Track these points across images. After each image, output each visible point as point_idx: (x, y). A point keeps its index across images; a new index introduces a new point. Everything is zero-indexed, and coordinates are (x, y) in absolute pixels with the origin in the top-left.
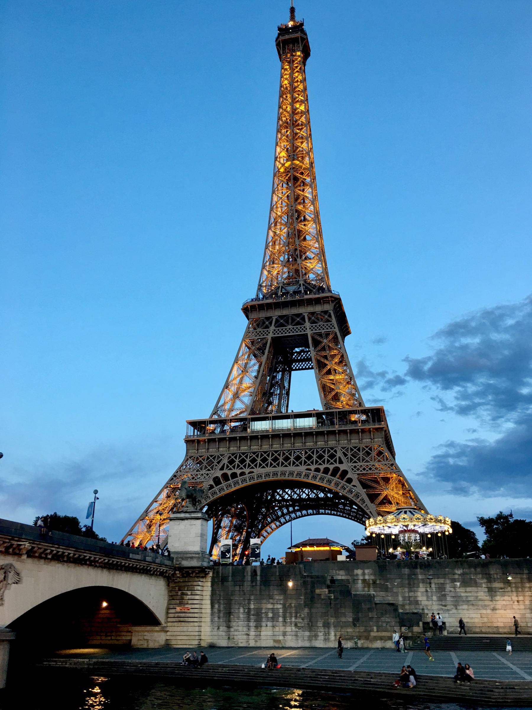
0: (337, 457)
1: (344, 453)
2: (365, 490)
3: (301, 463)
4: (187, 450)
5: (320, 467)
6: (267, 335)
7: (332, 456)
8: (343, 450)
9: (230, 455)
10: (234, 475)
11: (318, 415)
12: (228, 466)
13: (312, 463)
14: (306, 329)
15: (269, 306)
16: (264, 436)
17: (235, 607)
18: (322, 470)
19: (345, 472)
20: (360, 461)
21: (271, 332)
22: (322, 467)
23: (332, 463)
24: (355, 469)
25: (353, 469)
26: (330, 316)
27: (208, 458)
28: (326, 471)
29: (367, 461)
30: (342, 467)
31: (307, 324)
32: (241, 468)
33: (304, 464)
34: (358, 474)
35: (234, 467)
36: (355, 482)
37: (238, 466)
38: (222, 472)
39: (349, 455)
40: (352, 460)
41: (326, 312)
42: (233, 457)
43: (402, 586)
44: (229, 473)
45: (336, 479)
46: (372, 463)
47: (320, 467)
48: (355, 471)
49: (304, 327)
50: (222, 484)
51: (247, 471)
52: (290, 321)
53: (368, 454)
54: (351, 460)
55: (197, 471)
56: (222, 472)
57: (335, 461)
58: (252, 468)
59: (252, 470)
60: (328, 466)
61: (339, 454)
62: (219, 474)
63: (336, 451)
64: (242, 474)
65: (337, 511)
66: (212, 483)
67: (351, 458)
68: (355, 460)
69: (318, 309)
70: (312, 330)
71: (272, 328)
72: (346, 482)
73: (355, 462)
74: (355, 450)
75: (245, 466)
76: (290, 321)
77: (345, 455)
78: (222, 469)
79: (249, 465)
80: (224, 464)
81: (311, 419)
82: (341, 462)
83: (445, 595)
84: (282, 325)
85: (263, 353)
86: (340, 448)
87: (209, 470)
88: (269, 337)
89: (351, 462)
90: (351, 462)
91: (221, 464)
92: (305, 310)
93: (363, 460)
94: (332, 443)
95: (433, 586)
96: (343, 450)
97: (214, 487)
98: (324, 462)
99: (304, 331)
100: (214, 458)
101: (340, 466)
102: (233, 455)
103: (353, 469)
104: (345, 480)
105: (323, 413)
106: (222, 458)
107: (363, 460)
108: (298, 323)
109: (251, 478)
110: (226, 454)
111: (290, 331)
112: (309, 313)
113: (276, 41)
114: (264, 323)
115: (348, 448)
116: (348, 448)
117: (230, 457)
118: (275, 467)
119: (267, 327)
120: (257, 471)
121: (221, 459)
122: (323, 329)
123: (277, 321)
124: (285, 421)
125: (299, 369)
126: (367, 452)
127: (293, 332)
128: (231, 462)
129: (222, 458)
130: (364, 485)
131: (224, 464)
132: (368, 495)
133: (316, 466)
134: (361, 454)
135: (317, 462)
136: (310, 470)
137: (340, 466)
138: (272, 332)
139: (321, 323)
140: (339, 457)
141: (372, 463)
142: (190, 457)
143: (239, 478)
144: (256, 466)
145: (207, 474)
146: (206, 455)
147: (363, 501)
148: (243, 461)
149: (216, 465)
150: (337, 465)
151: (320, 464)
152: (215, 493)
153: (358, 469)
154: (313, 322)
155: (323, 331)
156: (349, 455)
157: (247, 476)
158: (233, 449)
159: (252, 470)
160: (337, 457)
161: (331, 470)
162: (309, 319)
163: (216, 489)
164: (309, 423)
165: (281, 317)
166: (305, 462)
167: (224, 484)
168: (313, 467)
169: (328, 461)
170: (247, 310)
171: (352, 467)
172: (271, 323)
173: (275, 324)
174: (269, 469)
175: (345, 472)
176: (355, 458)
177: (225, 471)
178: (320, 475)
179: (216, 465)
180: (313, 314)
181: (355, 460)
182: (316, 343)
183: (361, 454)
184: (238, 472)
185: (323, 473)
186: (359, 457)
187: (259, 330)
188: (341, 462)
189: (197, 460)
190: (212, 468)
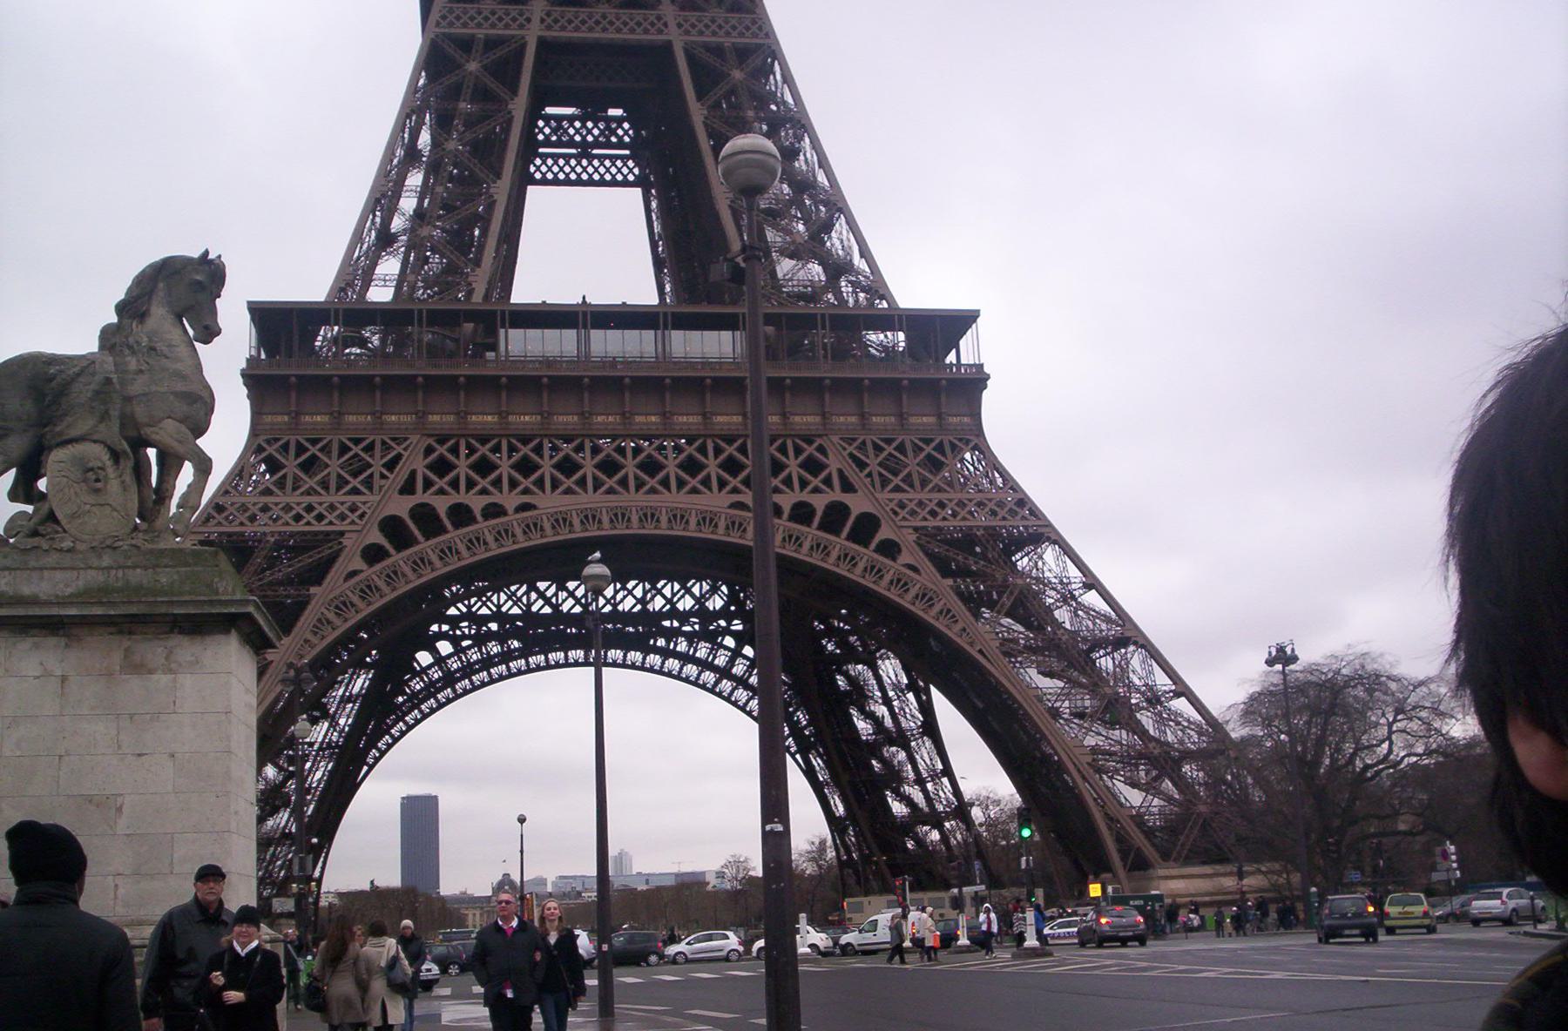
1: (851, 455)
2: (950, 582)
3: (706, 482)
4: (257, 414)
6: (521, 27)
7: (813, 466)
8: (850, 449)
9: (431, 441)
10: (461, 515)
12: (428, 484)
14: (666, 25)
18: (787, 510)
20: (912, 486)
23: (816, 490)
24: (903, 513)
25: (896, 513)
27: (344, 449)
28: (802, 513)
30: (858, 504)
32: (484, 492)
33: (720, 490)
34: (916, 529)
35: (455, 484)
38: (410, 502)
39: (873, 463)
40: (885, 482)
42: (442, 450)
44: (441, 505)
45: (839, 543)
48: (904, 519)
49: (659, 18)
50: (415, 542)
51: (510, 500)
53: (935, 465)
54: (885, 482)
55: (307, 493)
56: (410, 502)
57: (828, 481)
58: (526, 491)
59: (526, 499)
60: (805, 496)
61: (834, 464)
62: (401, 507)
63: (821, 449)
67: (880, 475)
68: (897, 481)
70: (687, 33)
72: (878, 550)
73: (897, 489)
75: (497, 483)
77: (861, 465)
78: (408, 488)
80: (413, 474)
82: (848, 487)
85: (514, 91)
86: (835, 439)
88: (532, 36)
89: (883, 487)
90: (883, 487)
91: (400, 475)
94: (806, 420)
96: (850, 449)
97: (386, 555)
99: (660, 32)
100: (370, 448)
101: (847, 499)
102: (442, 441)
103: (896, 513)
104: (873, 545)
106: (399, 449)
107: (924, 482)
110: (414, 439)
115: (864, 443)
116: (864, 443)
117: (429, 450)
118: (611, 491)
120: (549, 502)
121: (398, 457)
122: (728, 34)
124: (632, 335)
125: (556, 182)
126: (929, 456)
127: (619, 31)
128: (442, 467)
129: (399, 449)
131: (413, 474)
134: (912, 464)
137: (847, 499)
140: (840, 472)
142: (268, 442)
145: (353, 509)
149: (383, 476)
150: (837, 495)
152: (392, 576)
153: (913, 513)
155: (727, 42)
157: (513, 518)
158: (441, 419)
159: (526, 499)
161: (819, 513)
163: (397, 558)
167: (426, 546)
169: (804, 484)
171: (892, 505)
174: (588, 499)
175: (865, 528)
176: (896, 474)
177: (420, 497)
179: (383, 476)
181: (897, 481)
183: (912, 464)
184: (477, 503)
185: (792, 518)
186: (909, 475)
188: (848, 487)
189: (298, 455)
190: (368, 483)
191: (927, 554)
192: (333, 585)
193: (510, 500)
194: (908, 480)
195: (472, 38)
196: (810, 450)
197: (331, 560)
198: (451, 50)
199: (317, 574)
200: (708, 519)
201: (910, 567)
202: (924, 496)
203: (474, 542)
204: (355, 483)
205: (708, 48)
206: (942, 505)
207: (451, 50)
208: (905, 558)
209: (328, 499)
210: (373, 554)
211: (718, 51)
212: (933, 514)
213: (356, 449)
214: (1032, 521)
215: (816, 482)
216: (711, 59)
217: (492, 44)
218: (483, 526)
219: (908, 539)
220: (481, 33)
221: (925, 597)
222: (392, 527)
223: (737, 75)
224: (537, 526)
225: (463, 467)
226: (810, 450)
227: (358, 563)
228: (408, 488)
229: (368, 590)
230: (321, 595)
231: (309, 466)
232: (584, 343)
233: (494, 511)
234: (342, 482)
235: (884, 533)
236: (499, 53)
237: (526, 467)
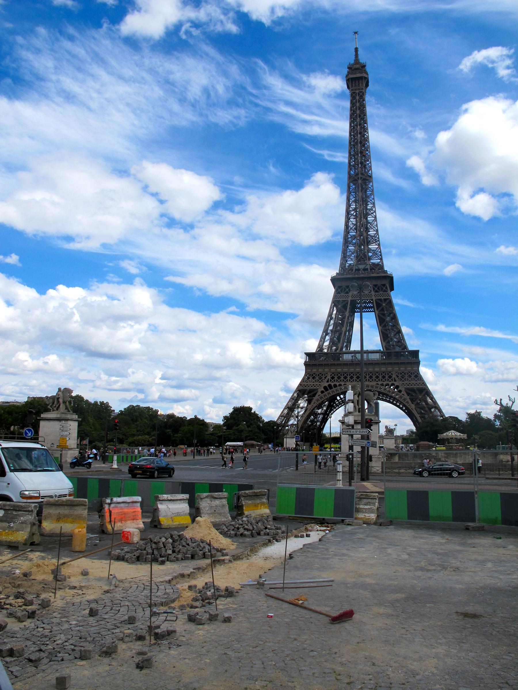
3: (373, 380)
7: (390, 377)
10: (335, 386)
11: (382, 352)
12: (331, 381)
13: (379, 380)
22: (385, 383)
26: (387, 288)
30: (396, 384)
35: (334, 381)
36: (403, 392)
37: (337, 380)
38: (328, 383)
41: (384, 285)
44: (332, 384)
46: (412, 382)
51: (343, 383)
53: (410, 376)
54: (401, 379)
56: (328, 383)
57: (392, 380)
61: (394, 376)
62: (326, 384)
63: (392, 374)
64: (340, 385)
66: (323, 389)
69: (379, 283)
75: (341, 381)
77: (398, 377)
78: (328, 382)
79: (343, 380)
81: (378, 354)
82: (395, 381)
91: (326, 380)
93: (408, 380)
94: (390, 369)
98: (386, 380)
100: (322, 375)
112: (374, 285)
113: (346, 77)
117: (331, 375)
128: (333, 378)
130: (408, 394)
132: (410, 398)
135: (382, 380)
139: (381, 293)
141: (412, 382)
143: (338, 388)
144: (347, 380)
146: (317, 373)
147: (407, 402)
148: (339, 378)
152: (325, 395)
154: (376, 291)
156: (400, 376)
163: (326, 393)
164: (377, 356)
166: (375, 380)
167: (330, 391)
168: (380, 383)
169: (388, 380)
177: (330, 383)
182: (378, 305)
183: (406, 376)
184: (338, 384)
190: (322, 381)
191: (406, 392)
192: (317, 396)
193: (343, 383)
194: (405, 379)
196: (390, 374)
197: (316, 394)
199: (314, 395)
200: (372, 386)
202: (407, 382)
208: (402, 393)
209: (316, 383)
210: (322, 392)
211: (380, 300)
215: (390, 380)
216: (379, 302)
219: (404, 389)
221: (405, 400)
222: (325, 388)
223: (384, 305)
226: (390, 374)
227: (320, 394)
228: (328, 382)
229: (321, 398)
230: (315, 398)
231: (313, 378)
233: (340, 385)
234: (318, 380)
235: (400, 389)
236: (344, 303)
237: (345, 378)
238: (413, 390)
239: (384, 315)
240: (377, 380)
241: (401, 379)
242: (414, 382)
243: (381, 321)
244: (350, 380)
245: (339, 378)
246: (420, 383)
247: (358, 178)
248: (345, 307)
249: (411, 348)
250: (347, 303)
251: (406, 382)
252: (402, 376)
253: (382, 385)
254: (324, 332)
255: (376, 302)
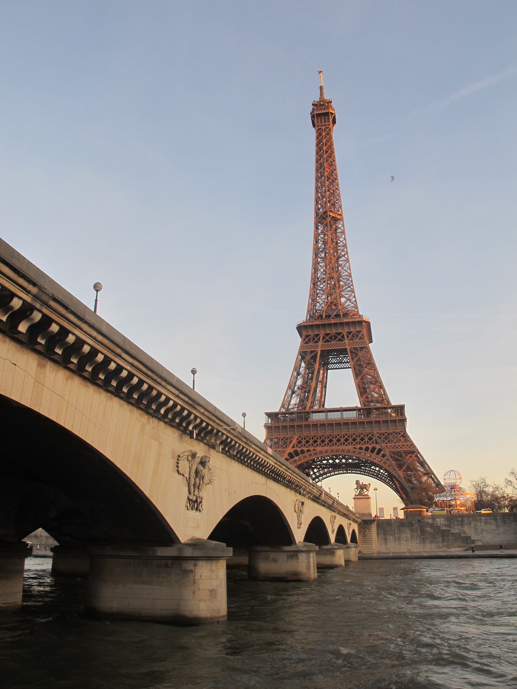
0: (374, 440)
3: (349, 443)
5: (362, 446)
7: (370, 439)
8: (378, 435)
10: (302, 452)
11: (359, 410)
12: (297, 445)
13: (357, 443)
15: (317, 326)
16: (322, 425)
17: (388, 537)
19: (380, 450)
21: (320, 346)
22: (364, 447)
23: (371, 444)
26: (363, 335)
27: (282, 439)
28: (367, 449)
29: (395, 443)
30: (378, 447)
31: (346, 341)
32: (307, 447)
35: (302, 446)
37: (305, 445)
41: (359, 332)
43: (458, 525)
44: (299, 450)
45: (374, 455)
47: (362, 446)
51: (311, 448)
52: (333, 338)
57: (373, 442)
58: (315, 447)
60: (368, 445)
63: (372, 435)
64: (309, 451)
65: (361, 471)
68: (386, 441)
71: (320, 343)
73: (387, 443)
74: (386, 434)
75: (309, 445)
76: (333, 338)
77: (379, 438)
78: (293, 447)
79: (312, 445)
81: (355, 412)
82: (377, 443)
83: (477, 529)
84: (327, 341)
85: (315, 362)
87: (284, 448)
92: (345, 331)
95: (472, 525)
96: (378, 435)
98: (365, 443)
100: (287, 439)
105: (362, 409)
108: (340, 340)
109: (316, 454)
111: (334, 345)
112: (348, 332)
114: (314, 339)
117: (298, 439)
118: (331, 446)
119: (316, 342)
120: (319, 449)
123: (324, 338)
128: (300, 442)
133: (360, 446)
135: (360, 443)
136: (355, 448)
138: (320, 347)
140: (376, 440)
145: (283, 451)
147: (394, 469)
148: (307, 442)
150: (374, 445)
151: (363, 444)
153: (389, 448)
155: (358, 347)
160: (374, 440)
162: (348, 337)
164: (353, 415)
165: (327, 335)
168: (358, 446)
170: (300, 328)
172: (319, 339)
173: (323, 340)
175: (380, 450)
177: (295, 449)
178: (363, 451)
180: (349, 333)
181: (386, 441)
184: (305, 449)
187: (310, 344)
190: (286, 446)
191: (391, 456)
193: (311, 448)
195: (307, 352)
198: (304, 355)
201: (387, 460)
203: (305, 457)
204: (284, 446)
205: (354, 348)
206: (395, 446)
207: (304, 355)
208: (386, 458)
212: (393, 448)
213: (285, 439)
214: (413, 449)
215: (370, 442)
216: (354, 351)
217: (312, 352)
218: (306, 453)
219: (388, 453)
220: (309, 350)
224: (316, 454)
225: (304, 441)
232: (326, 416)
233: (309, 451)
235: (382, 452)
238: (399, 454)
239: (360, 365)
240: (354, 443)
241: (384, 441)
242: (399, 444)
243: (358, 374)
244: (320, 445)
245: (307, 442)
246: (407, 445)
247: (327, 216)
248: (314, 358)
249: (394, 403)
250: (317, 353)
251: (390, 444)
252: (386, 437)
253: (361, 448)
254: (289, 387)
255: (350, 351)
